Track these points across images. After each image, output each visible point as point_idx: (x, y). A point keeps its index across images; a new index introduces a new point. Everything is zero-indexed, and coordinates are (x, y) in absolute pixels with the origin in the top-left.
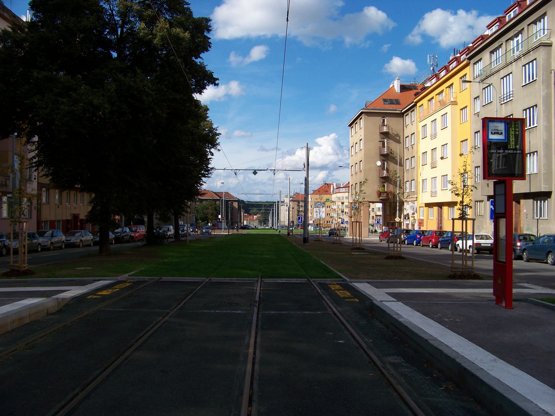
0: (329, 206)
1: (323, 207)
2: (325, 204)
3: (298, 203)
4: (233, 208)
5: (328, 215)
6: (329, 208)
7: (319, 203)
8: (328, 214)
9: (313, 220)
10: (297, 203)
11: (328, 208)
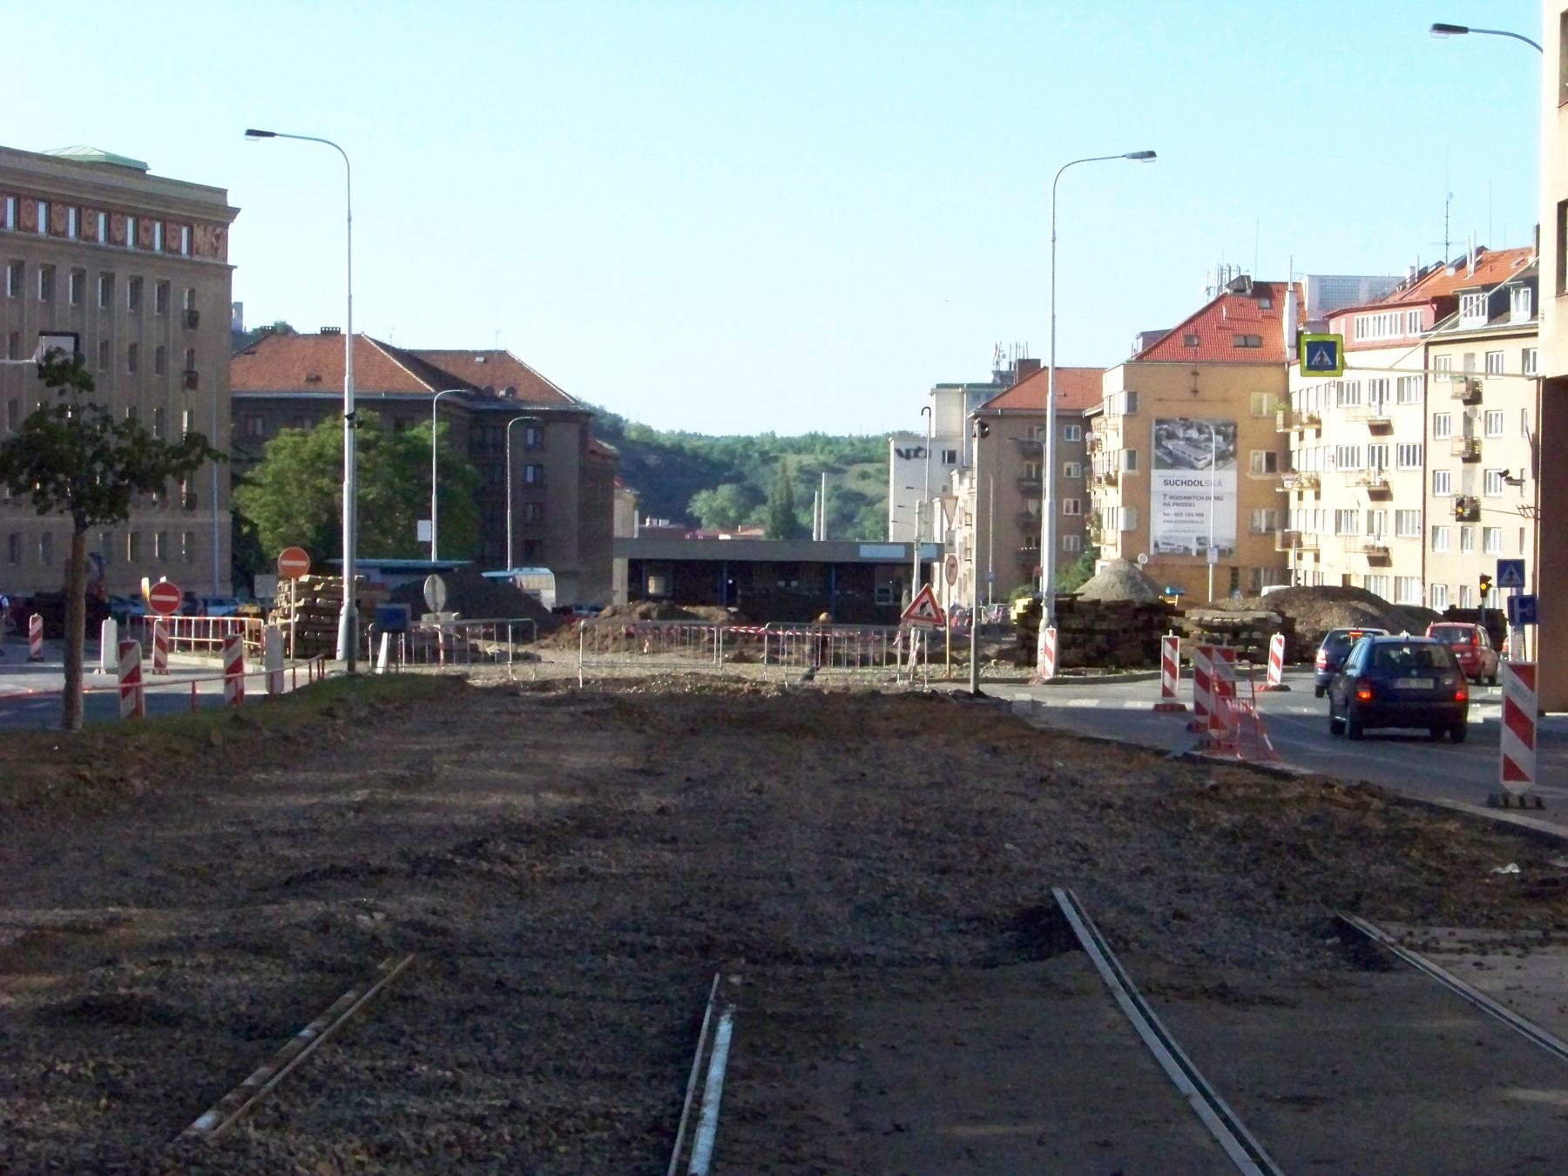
1: (1222, 457)
2: (1235, 435)
7: (1194, 434)
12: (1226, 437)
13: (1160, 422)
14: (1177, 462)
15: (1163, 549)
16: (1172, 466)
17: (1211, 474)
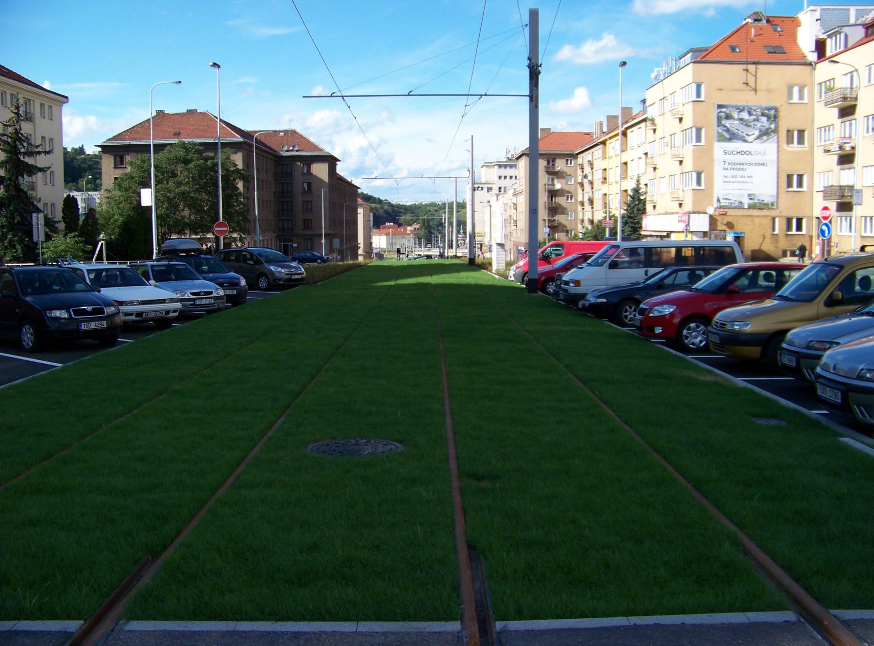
0: (801, 133)
1: (765, 133)
2: (775, 117)
3: (548, 163)
4: (312, 182)
5: (790, 185)
6: (801, 141)
7: (745, 115)
8: (789, 177)
9: (711, 211)
10: (546, 162)
11: (790, 141)
12: (769, 118)
13: (720, 106)
14: (733, 136)
15: (724, 203)
16: (730, 140)
17: (756, 146)
